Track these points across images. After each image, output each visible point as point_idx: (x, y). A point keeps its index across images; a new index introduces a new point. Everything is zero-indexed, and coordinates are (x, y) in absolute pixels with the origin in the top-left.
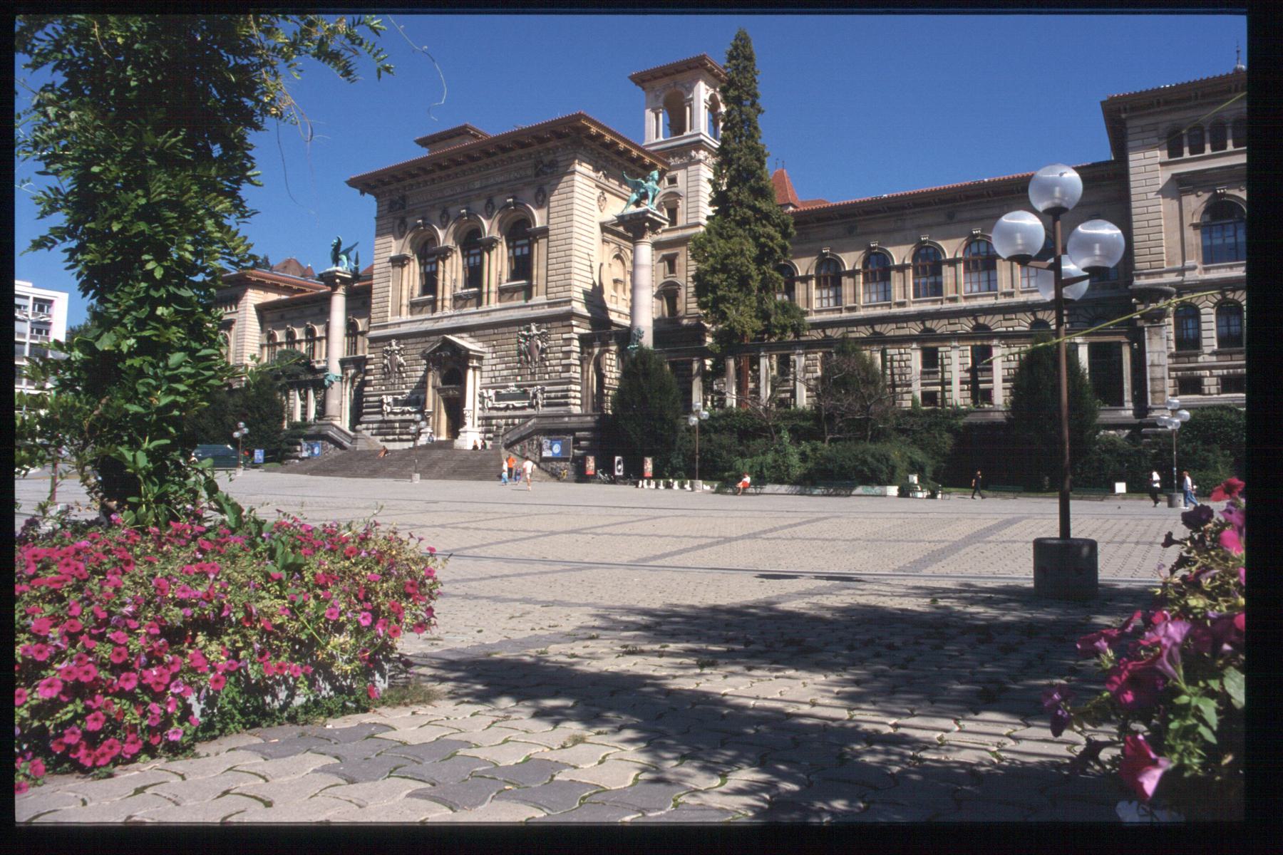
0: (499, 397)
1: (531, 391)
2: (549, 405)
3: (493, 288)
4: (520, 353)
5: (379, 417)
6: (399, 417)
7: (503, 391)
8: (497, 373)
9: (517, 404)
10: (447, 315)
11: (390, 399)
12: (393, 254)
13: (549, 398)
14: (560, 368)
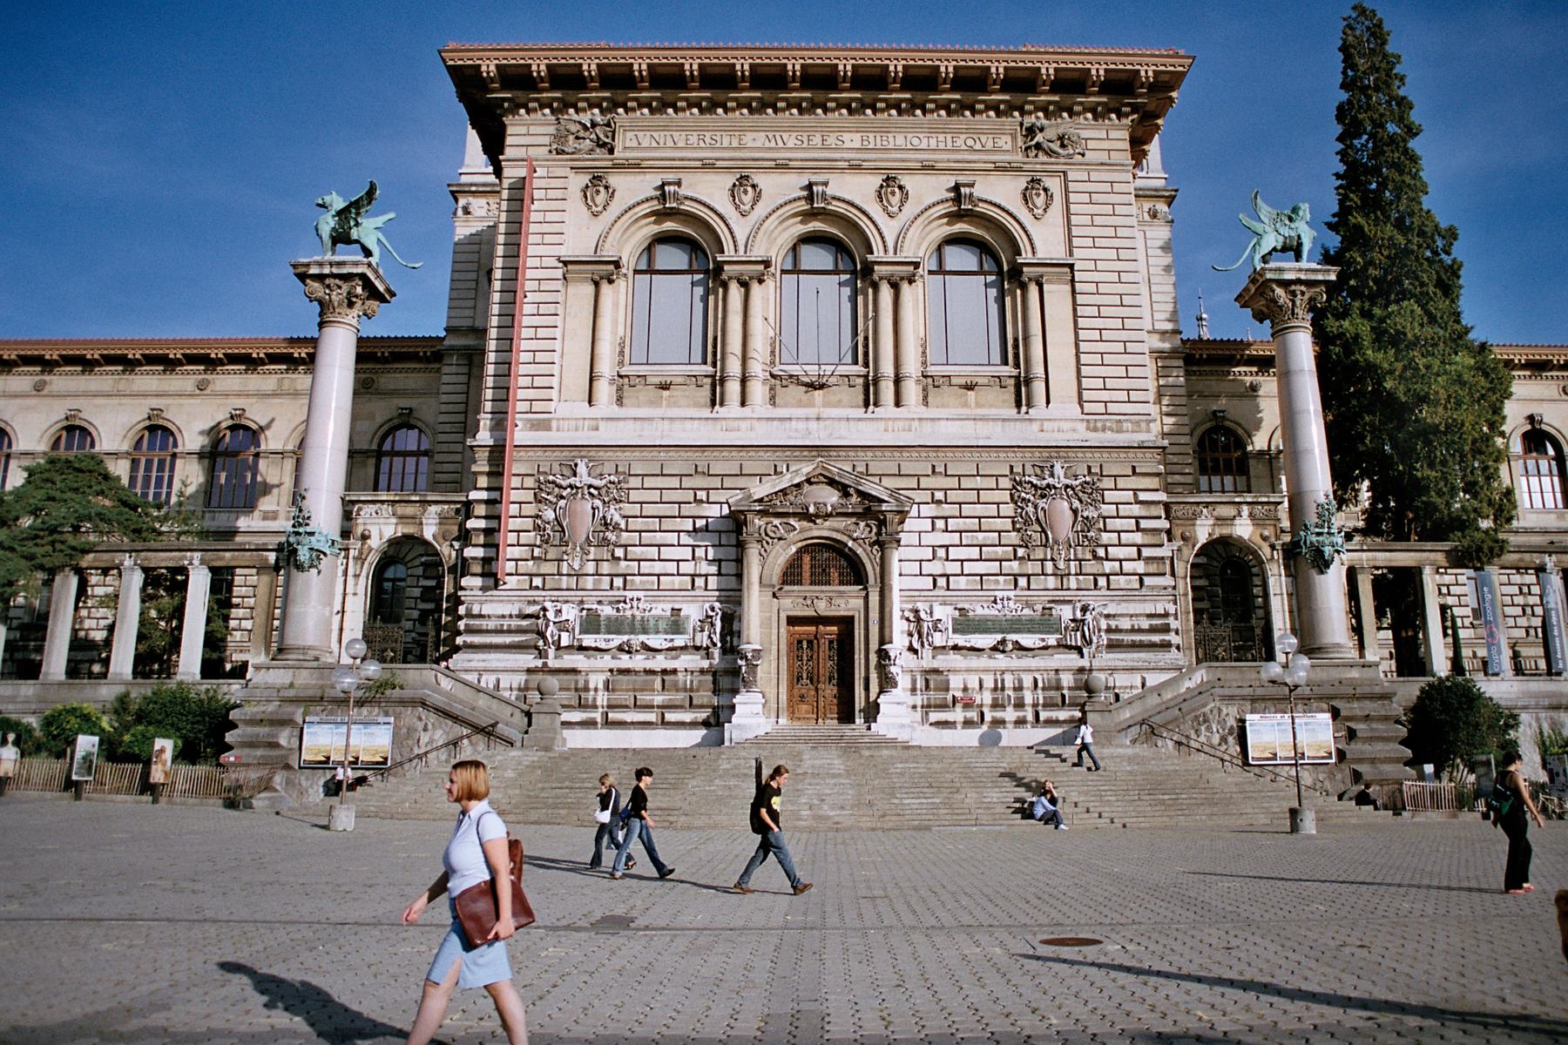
0: (965, 623)
1: (1066, 613)
2: (1113, 646)
3: (912, 367)
4: (1021, 523)
5: (529, 660)
6: (607, 661)
7: (980, 611)
8: (954, 568)
9: (1027, 640)
10: (753, 421)
11: (570, 613)
12: (565, 252)
13: (1118, 630)
14: (1140, 567)
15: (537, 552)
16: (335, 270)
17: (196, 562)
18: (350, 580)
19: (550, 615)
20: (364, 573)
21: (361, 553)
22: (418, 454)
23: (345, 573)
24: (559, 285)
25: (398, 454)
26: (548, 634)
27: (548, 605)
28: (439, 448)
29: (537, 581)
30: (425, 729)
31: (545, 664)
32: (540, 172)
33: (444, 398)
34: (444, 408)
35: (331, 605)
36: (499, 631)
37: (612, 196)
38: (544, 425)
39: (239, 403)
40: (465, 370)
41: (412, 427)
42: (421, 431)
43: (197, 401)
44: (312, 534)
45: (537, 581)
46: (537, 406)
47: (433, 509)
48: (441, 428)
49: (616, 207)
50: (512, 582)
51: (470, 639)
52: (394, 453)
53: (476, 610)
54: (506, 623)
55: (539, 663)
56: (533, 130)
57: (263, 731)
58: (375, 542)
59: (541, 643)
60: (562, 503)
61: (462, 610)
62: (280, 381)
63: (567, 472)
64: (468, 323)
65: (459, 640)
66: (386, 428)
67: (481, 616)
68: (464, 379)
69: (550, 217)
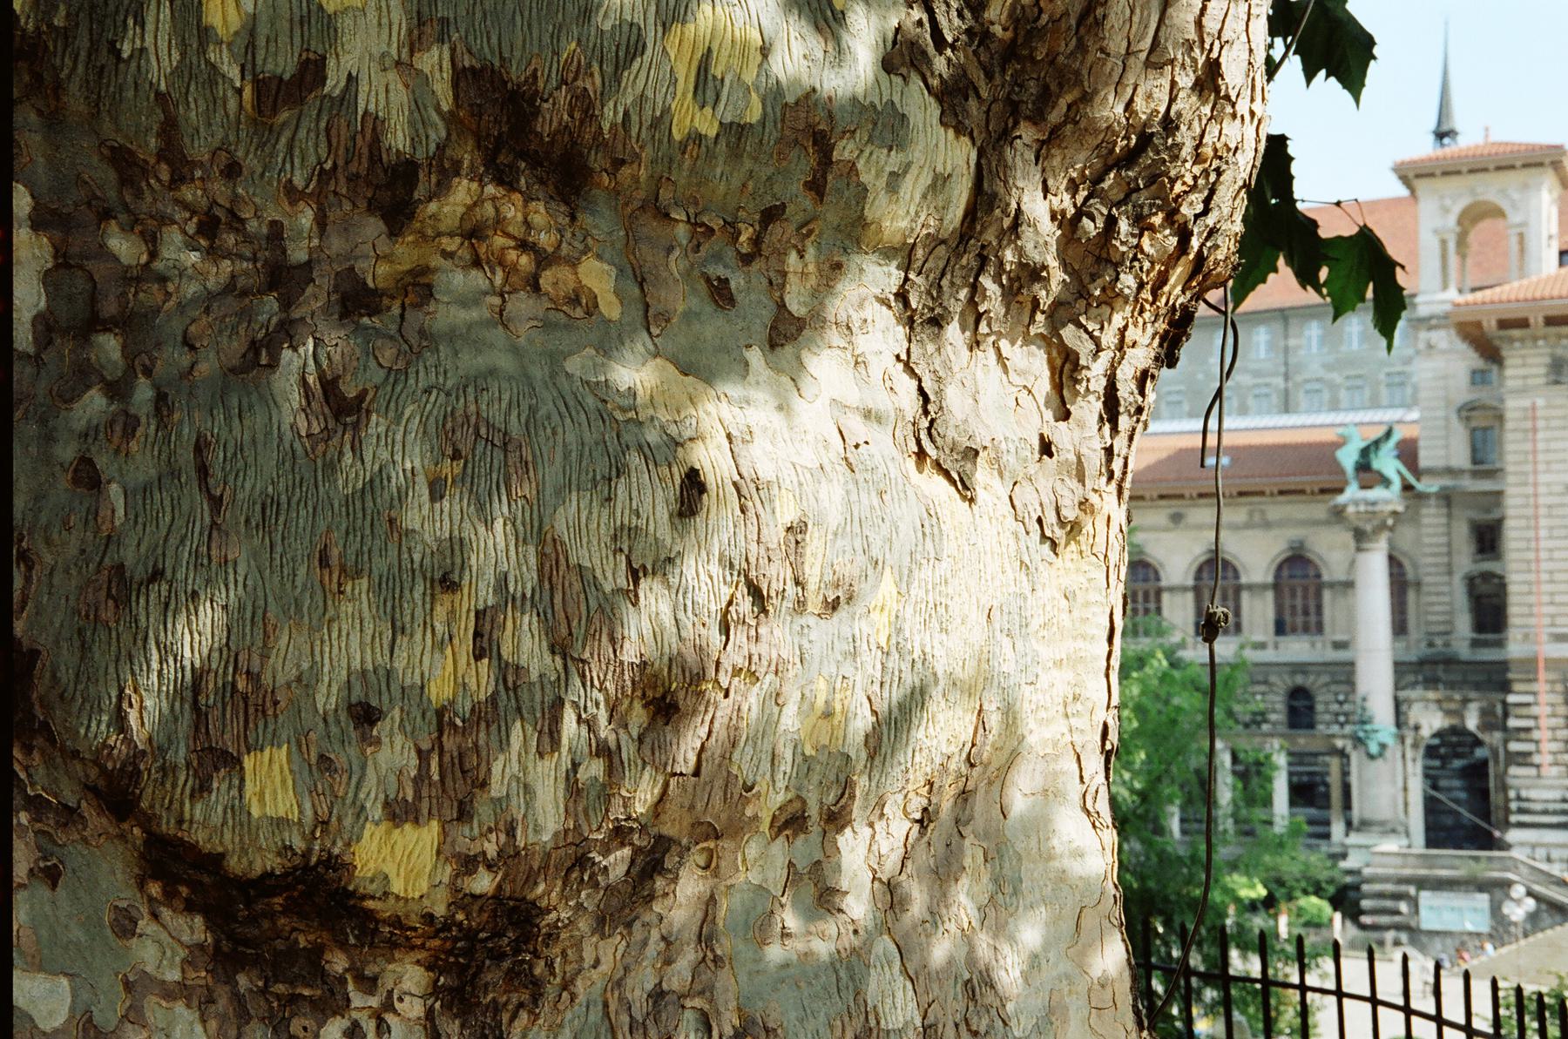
18: (1409, 764)
23: (1404, 756)
35: (1394, 782)
36: (1545, 812)
40: (1444, 511)
43: (1171, 535)
53: (1524, 794)
54: (1551, 807)
56: (1530, 361)
57: (1389, 904)
58: (1426, 732)
61: (1512, 794)
62: (1251, 514)
67: (1528, 800)
68: (1444, 520)
69: (1553, 445)
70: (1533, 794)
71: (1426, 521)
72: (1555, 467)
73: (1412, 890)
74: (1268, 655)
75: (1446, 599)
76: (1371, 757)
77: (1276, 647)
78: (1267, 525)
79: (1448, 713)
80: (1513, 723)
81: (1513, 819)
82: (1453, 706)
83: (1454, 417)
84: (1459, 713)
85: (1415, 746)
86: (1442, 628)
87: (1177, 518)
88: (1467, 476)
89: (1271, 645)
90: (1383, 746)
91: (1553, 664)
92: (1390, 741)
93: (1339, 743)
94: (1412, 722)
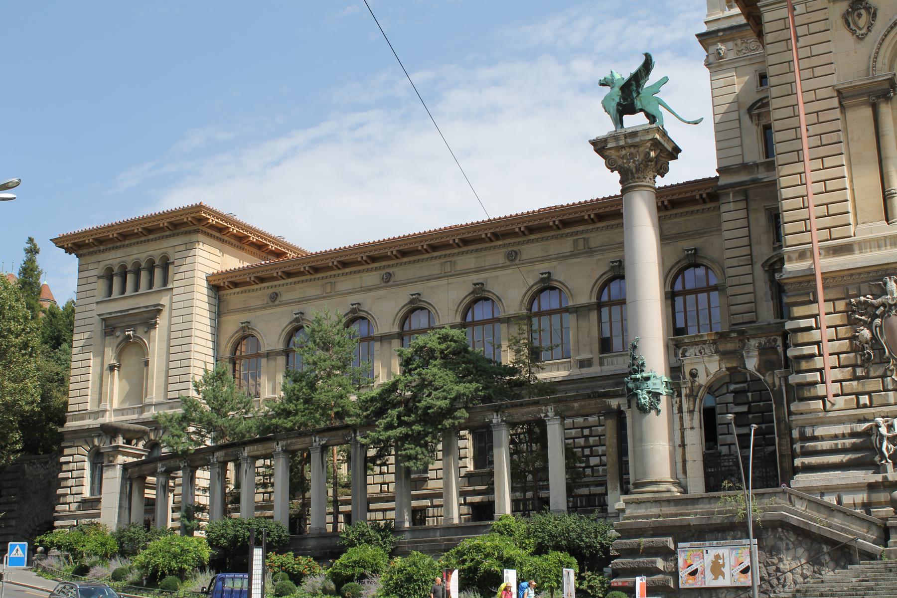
15: (859, 372)
16: (629, 141)
17: (550, 414)
19: (883, 430)
20: (697, 409)
21: (692, 390)
22: (708, 289)
23: (680, 410)
24: (837, 113)
25: (690, 292)
26: (884, 449)
27: (880, 420)
28: (729, 282)
29: (865, 399)
30: (788, 549)
31: (885, 478)
32: (799, 9)
33: (727, 235)
34: (728, 244)
37: (874, 16)
38: (846, 249)
39: (544, 267)
40: (742, 205)
41: (697, 266)
42: (707, 268)
44: (648, 379)
45: (865, 399)
46: (836, 232)
47: (753, 343)
48: (729, 263)
49: (880, 26)
50: (840, 402)
51: (808, 460)
52: (685, 293)
53: (808, 432)
54: (840, 443)
55: (879, 478)
58: (702, 380)
59: (877, 459)
60: (878, 321)
61: (796, 434)
62: (575, 242)
63: (876, 291)
64: (738, 160)
65: (798, 462)
66: (675, 270)
67: (815, 438)
68: (743, 214)
69: (816, 50)
70: (820, 431)
71: (725, 217)
72: (818, 71)
73: (670, 542)
74: (594, 370)
75: (750, 288)
76: (643, 410)
77: (601, 364)
78: (590, 252)
79: (724, 355)
80: (792, 352)
81: (798, 462)
82: (730, 346)
83: (746, 119)
84: (738, 355)
85: (692, 396)
86: (747, 317)
87: (513, 256)
88: (761, 169)
89: (596, 361)
90: (656, 395)
91: (831, 279)
92: (663, 390)
93: (614, 403)
94: (687, 370)
